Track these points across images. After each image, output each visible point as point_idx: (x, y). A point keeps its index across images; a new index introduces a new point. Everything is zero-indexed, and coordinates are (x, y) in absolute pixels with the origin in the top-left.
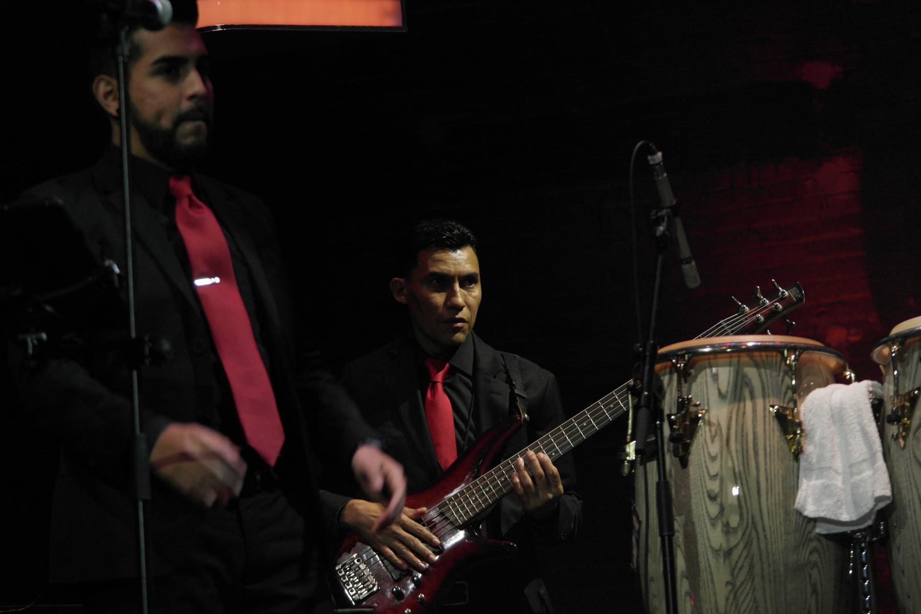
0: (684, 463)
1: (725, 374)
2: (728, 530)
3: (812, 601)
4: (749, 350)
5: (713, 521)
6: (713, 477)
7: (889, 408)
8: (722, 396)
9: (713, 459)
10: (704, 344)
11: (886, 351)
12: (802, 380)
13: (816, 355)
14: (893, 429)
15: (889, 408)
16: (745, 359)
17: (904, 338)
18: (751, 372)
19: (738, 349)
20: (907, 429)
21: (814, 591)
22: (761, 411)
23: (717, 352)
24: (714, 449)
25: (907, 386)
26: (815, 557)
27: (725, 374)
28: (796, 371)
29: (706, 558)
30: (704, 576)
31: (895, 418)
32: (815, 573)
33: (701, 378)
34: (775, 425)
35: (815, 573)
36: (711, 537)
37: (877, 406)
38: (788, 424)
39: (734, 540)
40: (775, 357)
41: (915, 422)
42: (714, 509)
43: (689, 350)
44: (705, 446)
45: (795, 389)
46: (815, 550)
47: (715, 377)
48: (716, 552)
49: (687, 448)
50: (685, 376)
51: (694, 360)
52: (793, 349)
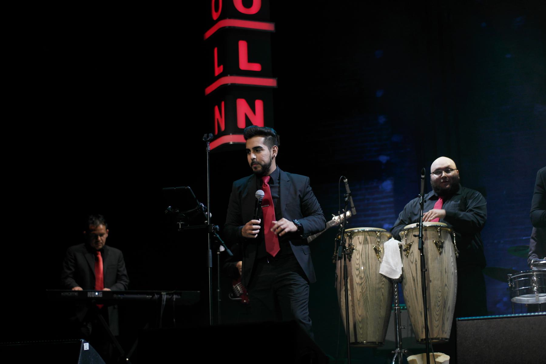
0: (350, 260)
1: (361, 237)
2: (361, 278)
3: (382, 297)
4: (367, 231)
5: (357, 276)
6: (357, 264)
7: (404, 248)
8: (360, 243)
9: (357, 259)
10: (356, 230)
11: (403, 233)
12: (381, 239)
13: (385, 233)
14: (404, 253)
15: (404, 248)
16: (366, 234)
17: (408, 230)
18: (368, 237)
19: (364, 231)
20: (408, 253)
21: (383, 295)
22: (370, 247)
23: (359, 232)
24: (358, 257)
25: (409, 242)
26: (383, 286)
27: (361, 237)
28: (380, 237)
29: (355, 285)
30: (354, 290)
31: (406, 250)
32: (383, 290)
33: (355, 238)
34: (374, 251)
35: (383, 290)
36: (357, 280)
37: (401, 247)
38: (377, 251)
39: (363, 281)
40: (374, 233)
41: (411, 251)
42: (357, 273)
43: (352, 231)
44: (355, 256)
45: (379, 242)
46: (383, 284)
47: (359, 238)
48: (357, 284)
49: (351, 257)
50: (351, 238)
51: (352, 234)
52: (379, 231)
